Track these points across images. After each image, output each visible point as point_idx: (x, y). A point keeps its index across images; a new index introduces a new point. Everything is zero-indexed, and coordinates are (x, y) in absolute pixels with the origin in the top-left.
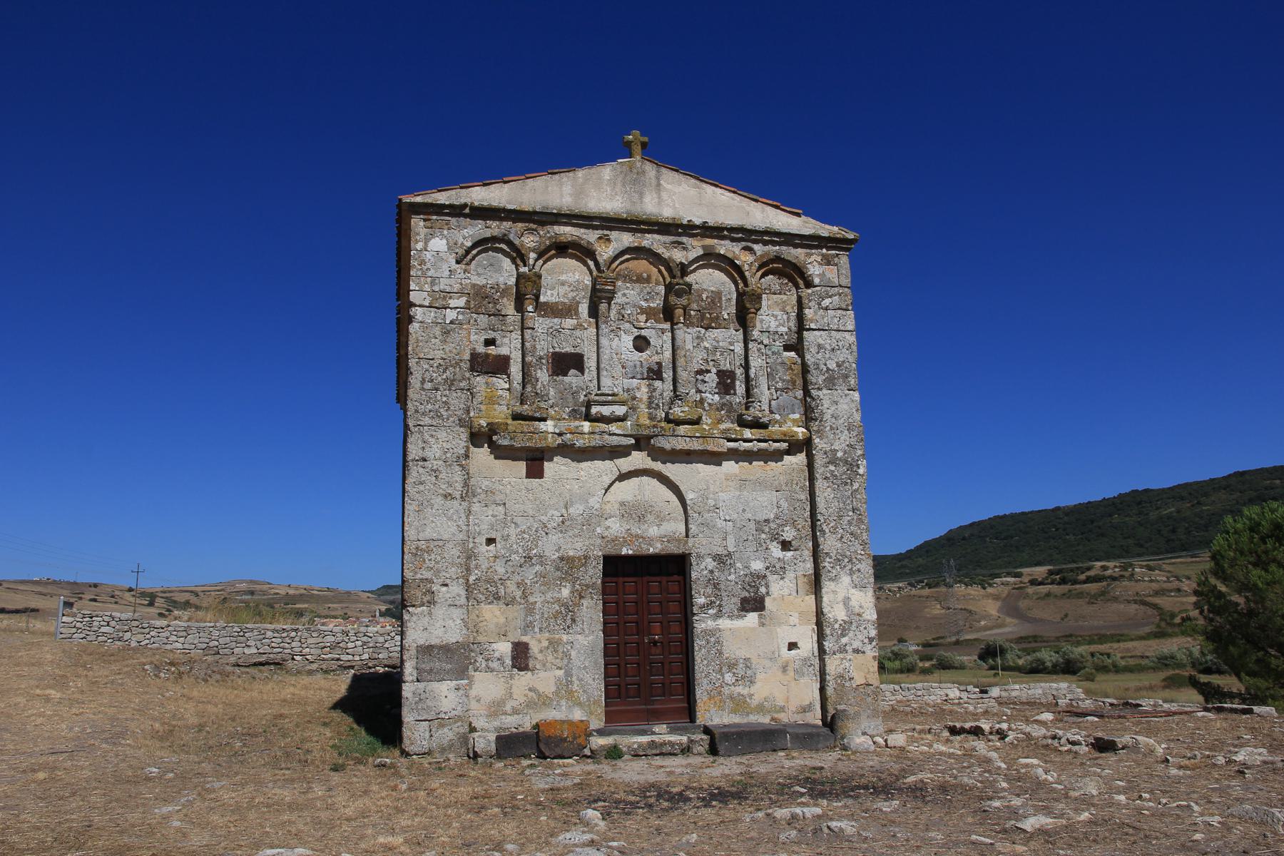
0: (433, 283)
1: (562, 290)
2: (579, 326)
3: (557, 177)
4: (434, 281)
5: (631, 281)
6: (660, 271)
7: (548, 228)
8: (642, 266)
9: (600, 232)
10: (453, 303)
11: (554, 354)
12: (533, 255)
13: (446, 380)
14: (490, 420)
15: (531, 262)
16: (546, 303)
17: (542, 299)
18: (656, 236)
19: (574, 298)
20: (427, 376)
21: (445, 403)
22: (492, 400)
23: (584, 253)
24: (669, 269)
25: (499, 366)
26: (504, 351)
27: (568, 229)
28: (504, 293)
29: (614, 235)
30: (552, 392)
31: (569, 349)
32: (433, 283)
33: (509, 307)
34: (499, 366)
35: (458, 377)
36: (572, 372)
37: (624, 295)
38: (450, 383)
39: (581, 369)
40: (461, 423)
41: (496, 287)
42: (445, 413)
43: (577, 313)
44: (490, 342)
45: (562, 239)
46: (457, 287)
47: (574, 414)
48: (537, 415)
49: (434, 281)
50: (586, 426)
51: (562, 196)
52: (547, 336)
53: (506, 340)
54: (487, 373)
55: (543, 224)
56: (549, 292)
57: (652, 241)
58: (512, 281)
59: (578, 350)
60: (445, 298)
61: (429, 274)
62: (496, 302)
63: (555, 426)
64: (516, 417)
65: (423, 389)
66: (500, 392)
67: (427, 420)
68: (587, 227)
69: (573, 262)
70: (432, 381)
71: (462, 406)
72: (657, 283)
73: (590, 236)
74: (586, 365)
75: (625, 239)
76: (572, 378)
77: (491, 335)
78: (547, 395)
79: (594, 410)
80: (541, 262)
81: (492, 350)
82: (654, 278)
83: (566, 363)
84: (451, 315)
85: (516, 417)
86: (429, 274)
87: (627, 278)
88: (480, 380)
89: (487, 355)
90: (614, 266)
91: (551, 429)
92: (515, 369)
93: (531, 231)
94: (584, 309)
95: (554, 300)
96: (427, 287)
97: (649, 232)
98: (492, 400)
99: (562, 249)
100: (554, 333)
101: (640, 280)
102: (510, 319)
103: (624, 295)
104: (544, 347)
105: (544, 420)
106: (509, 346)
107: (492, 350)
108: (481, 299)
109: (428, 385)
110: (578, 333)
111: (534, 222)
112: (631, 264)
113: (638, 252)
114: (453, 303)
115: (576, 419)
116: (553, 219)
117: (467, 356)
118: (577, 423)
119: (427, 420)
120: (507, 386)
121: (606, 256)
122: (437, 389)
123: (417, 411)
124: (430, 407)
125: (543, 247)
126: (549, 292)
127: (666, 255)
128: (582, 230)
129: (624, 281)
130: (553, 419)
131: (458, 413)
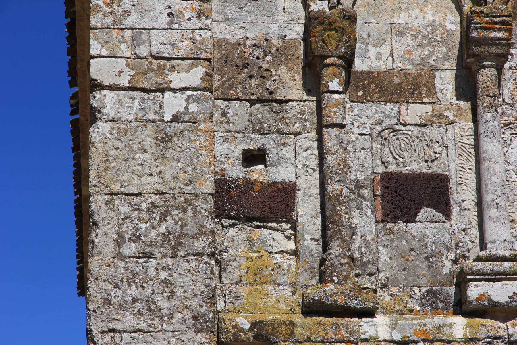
0: (135, 42)
1: (400, 45)
2: (437, 118)
4: (138, 34)
10: (177, 79)
11: (387, 177)
13: (166, 236)
14: (258, 317)
16: (367, 74)
17: (359, 65)
19: (424, 61)
20: (128, 228)
21: (166, 283)
22: (261, 276)
25: (275, 205)
26: (283, 173)
28: (282, 54)
30: (384, 255)
31: (416, 166)
32: (135, 42)
33: (290, 84)
34: (275, 205)
35: (191, 228)
36: (425, 212)
38: (175, 242)
39: (443, 206)
40: (199, 324)
41: (263, 45)
42: (164, 305)
43: (431, 91)
44: (254, 157)
46: (184, 48)
47: (432, 301)
48: (355, 303)
49: (138, 34)
50: (459, 326)
52: (368, 140)
53: (287, 152)
54: (249, 219)
56: (373, 51)
58: (296, 31)
59: (436, 168)
60: (160, 70)
61: (129, 22)
62: (264, 75)
63: (393, 327)
64: (312, 308)
65: (120, 256)
66: (278, 259)
67: (128, 320)
70: (137, 238)
71: (199, 288)
74: (454, 197)
76: (426, 226)
77: (256, 141)
78: (375, 261)
79: (475, 291)
81: (258, 173)
83: (410, 195)
84: (173, 104)
85: (312, 308)
86: (129, 22)
88: (236, 236)
89: (249, 184)
91: (384, 333)
92: (307, 210)
94: (446, 81)
95: (381, 65)
96: (125, 50)
98: (261, 276)
100: (387, 133)
102: (293, 109)
104: (364, 162)
105: (370, 313)
106: (293, 164)
107: (258, 173)
108: (235, 71)
109: (130, 248)
110: (434, 132)
114: (177, 79)
115: (435, 310)
117: (208, 186)
118: (439, 320)
119: (128, 320)
120: (291, 245)
122: (148, 256)
123: (107, 302)
124: (133, 291)
126: (373, 51)
130: (387, 311)
131: (194, 303)
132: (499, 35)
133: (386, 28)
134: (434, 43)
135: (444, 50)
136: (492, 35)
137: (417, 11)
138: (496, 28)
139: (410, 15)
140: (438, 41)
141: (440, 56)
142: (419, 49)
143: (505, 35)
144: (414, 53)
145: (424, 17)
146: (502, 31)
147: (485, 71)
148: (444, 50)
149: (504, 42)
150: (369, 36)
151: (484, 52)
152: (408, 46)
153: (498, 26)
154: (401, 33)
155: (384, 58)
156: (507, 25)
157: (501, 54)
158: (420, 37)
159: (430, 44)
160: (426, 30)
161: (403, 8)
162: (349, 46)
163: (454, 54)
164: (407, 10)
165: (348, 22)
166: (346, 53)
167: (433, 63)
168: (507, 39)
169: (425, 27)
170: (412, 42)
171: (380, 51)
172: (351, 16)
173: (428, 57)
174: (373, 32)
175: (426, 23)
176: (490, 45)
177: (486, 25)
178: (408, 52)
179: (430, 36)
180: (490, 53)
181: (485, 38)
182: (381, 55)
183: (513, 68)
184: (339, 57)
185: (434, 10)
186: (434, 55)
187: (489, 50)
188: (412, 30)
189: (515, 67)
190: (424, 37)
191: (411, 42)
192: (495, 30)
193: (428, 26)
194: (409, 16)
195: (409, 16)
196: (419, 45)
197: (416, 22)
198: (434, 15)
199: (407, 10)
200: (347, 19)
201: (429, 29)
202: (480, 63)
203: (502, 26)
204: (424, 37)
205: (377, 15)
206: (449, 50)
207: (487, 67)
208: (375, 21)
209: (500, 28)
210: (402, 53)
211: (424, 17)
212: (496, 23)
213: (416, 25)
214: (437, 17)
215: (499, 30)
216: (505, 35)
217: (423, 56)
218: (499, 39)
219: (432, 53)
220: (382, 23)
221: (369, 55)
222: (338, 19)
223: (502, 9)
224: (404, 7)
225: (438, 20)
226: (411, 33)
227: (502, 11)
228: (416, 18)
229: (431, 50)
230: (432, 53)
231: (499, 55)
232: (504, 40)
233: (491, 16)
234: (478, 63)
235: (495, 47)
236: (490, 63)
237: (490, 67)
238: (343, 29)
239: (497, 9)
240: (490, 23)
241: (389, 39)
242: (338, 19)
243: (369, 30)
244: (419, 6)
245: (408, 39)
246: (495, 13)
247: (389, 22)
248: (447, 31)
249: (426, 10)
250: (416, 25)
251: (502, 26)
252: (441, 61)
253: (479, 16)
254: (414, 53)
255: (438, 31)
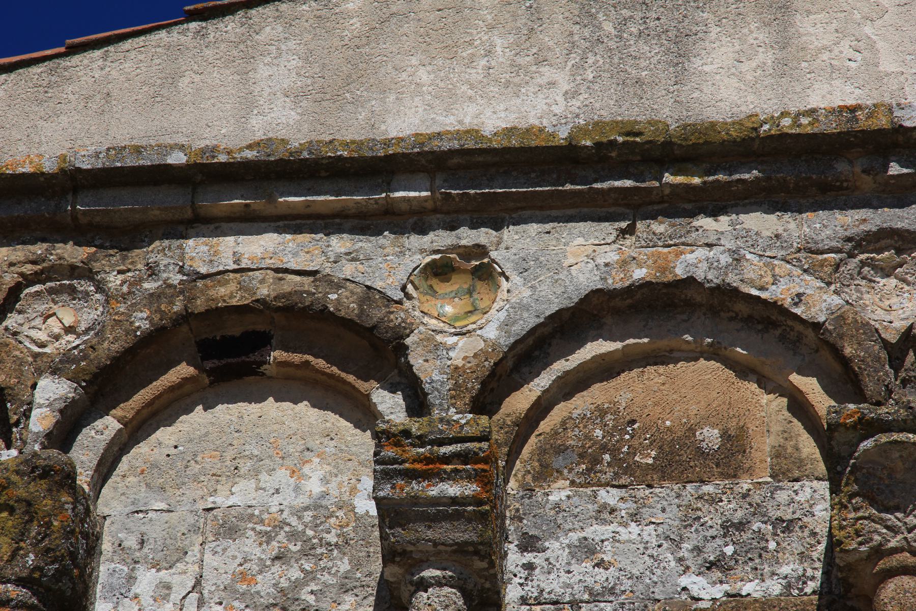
3: (230, 26)
5: (628, 473)
6: (799, 406)
7: (160, 253)
8: (693, 391)
9: (440, 239)
12: (52, 391)
15: (41, 421)
18: (761, 223)
23: (348, 353)
24: (845, 381)
27: (259, 247)
29: (513, 244)
37: (586, 550)
45: (228, 293)
51: (248, 104)
55: (126, 236)
57: (747, 249)
68: (365, 223)
69: (304, 417)
72: (786, 470)
73: (383, 264)
75: (578, 257)
80: (108, 426)
82: (762, 447)
87: (604, 460)
90: (520, 401)
93: (64, 280)
97: (716, 202)
99: (230, 350)
101: (679, 460)
103: (586, 550)
111: (79, 232)
112: (627, 391)
113: (661, 314)
116: (171, 201)
121: (461, 350)
125: (111, 346)
127: (819, 302)
128: (339, 243)
129: (589, 479)
132: (452, 489)
133: (191, 519)
134: (319, 551)
135: (344, 566)
136: (434, 492)
137: (282, 475)
138: (445, 471)
139: (262, 485)
140: (329, 544)
141: (331, 580)
142: (277, 568)
143: (470, 489)
144: (259, 578)
145: (297, 489)
146: (462, 478)
147: (425, 595)
148: (344, 566)
149: (470, 508)
150: (142, 543)
151: (418, 540)
152: (246, 560)
153: (449, 468)
154: (229, 529)
155: (176, 597)
156: (476, 464)
157: (466, 543)
158: (282, 536)
159: (307, 552)
160: (299, 518)
161: (243, 471)
162: (48, 550)
163: (370, 575)
164: (255, 473)
165: (44, 484)
166: (37, 568)
167: (311, 599)
168: (477, 501)
169: (298, 513)
170: (257, 551)
171: (168, 579)
172: (51, 468)
173: (297, 585)
174: (155, 532)
175: (302, 500)
176: (432, 520)
177: (418, 466)
178: (243, 576)
179: (310, 533)
180: (435, 544)
181: (415, 500)
182: (168, 587)
183: (532, 601)
184: (20, 582)
185: (328, 468)
186: (314, 579)
187: (430, 534)
188: (262, 522)
189: (536, 599)
190: (293, 536)
191: (257, 552)
192: (443, 477)
193: (307, 508)
194: (258, 489)
195: (258, 489)
196: (277, 558)
197: (277, 499)
198: (325, 481)
199: (255, 473)
200: (41, 477)
201: (308, 516)
202: (413, 575)
203: (460, 467)
204: (293, 536)
205: (170, 492)
206: (357, 565)
207: (431, 585)
208: (163, 506)
209: (456, 471)
210: (226, 579)
211: (297, 489)
212: (446, 459)
213: (274, 509)
214: (333, 485)
215: (454, 476)
216: (470, 489)
217: (284, 583)
218: (454, 500)
219: (309, 576)
220: (182, 511)
221: (135, 589)
222: (15, 478)
223: (463, 422)
224: (245, 466)
225: (334, 492)
226: (259, 528)
227: (462, 427)
228: (277, 491)
229: (308, 566)
230: (309, 576)
231: (461, 549)
232: (470, 505)
233: (433, 443)
234: (408, 577)
235: (446, 525)
236: (438, 573)
237: (439, 583)
238: (29, 504)
239: (448, 422)
240: (428, 460)
241: (197, 548)
242: (15, 478)
243: (143, 529)
244: (288, 462)
245: (249, 545)
246: (441, 432)
247: (201, 505)
248: (358, 518)
249: (306, 469)
250: (274, 509)
251: (460, 467)
252: (332, 593)
253: (397, 444)
254: (259, 578)
255: (333, 520)
